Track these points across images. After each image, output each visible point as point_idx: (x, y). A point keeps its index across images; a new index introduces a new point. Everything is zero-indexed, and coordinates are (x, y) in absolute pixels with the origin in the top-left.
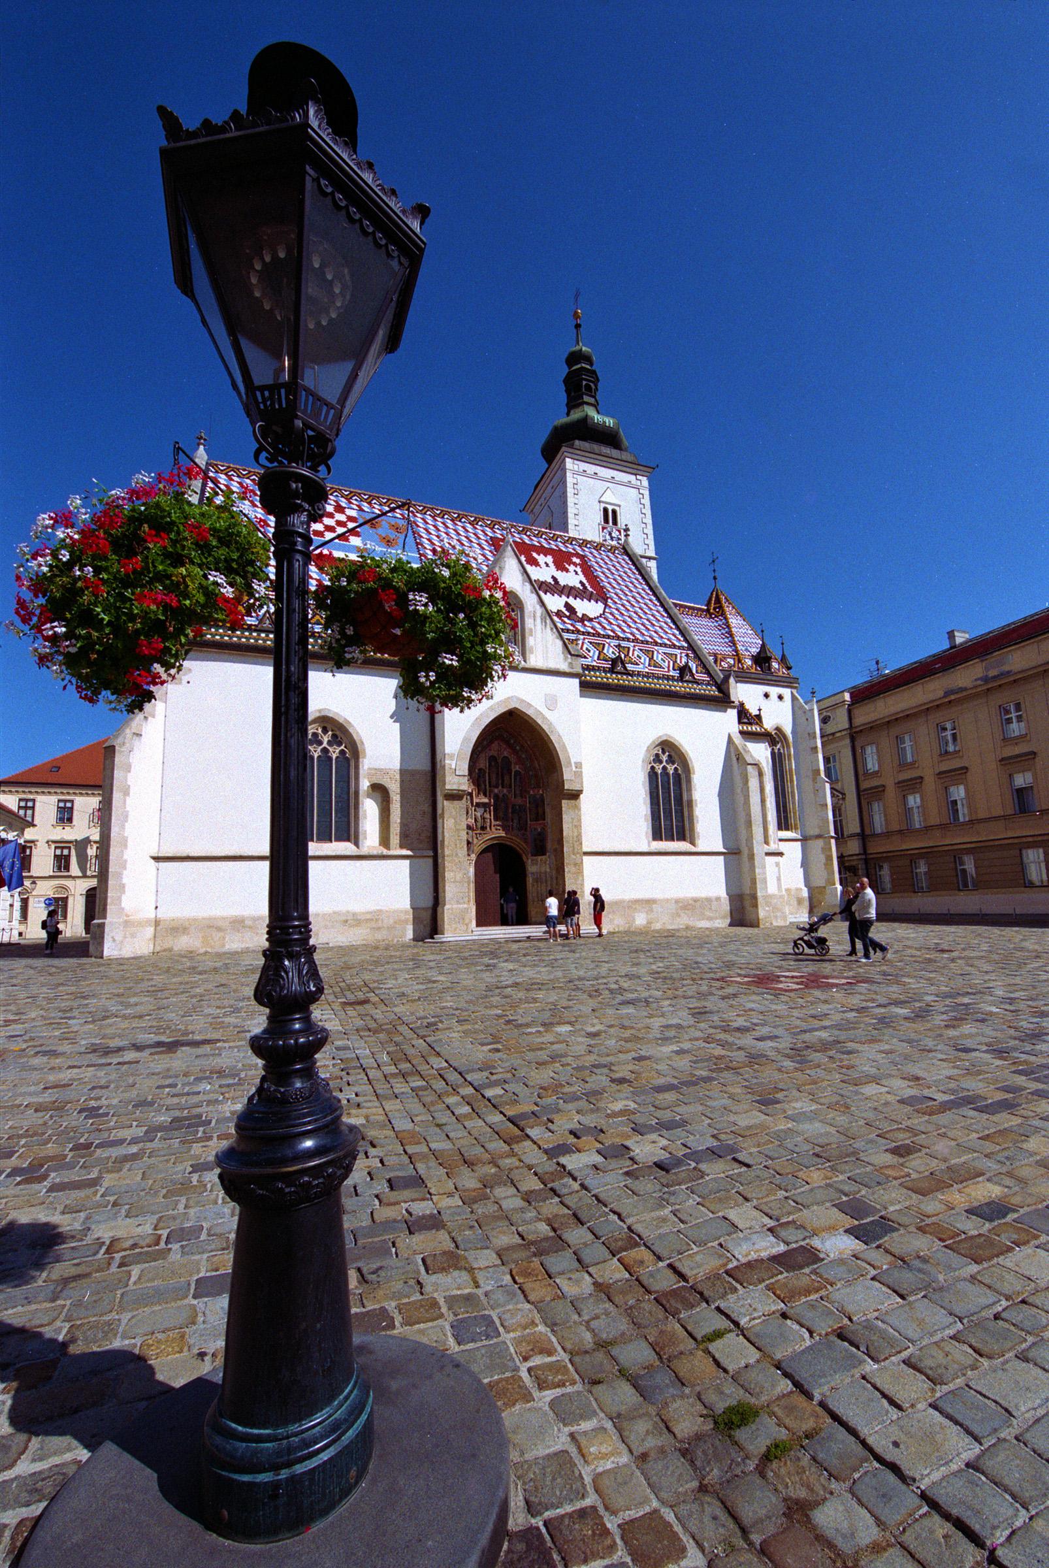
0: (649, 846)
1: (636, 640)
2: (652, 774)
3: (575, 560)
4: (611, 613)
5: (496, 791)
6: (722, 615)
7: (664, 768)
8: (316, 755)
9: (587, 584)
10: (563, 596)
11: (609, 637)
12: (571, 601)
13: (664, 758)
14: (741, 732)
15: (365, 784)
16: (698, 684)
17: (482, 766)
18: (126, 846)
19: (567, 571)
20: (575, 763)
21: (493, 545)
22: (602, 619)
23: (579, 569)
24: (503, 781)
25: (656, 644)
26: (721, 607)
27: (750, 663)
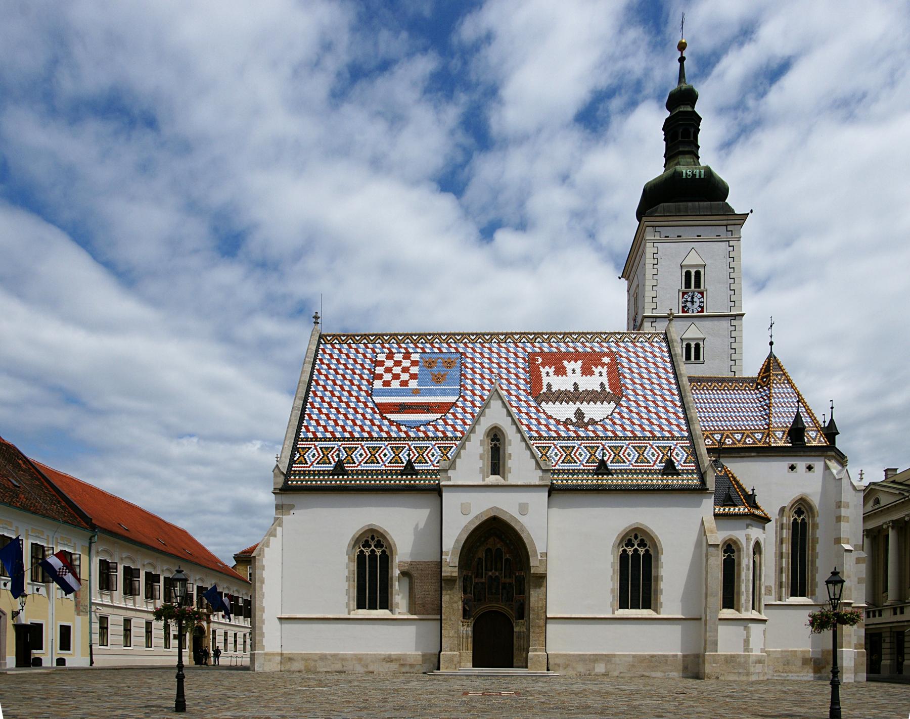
1: (635, 437)
3: (606, 360)
4: (619, 413)
5: (490, 573)
6: (766, 386)
8: (367, 554)
9: (607, 386)
10: (578, 403)
11: (607, 438)
12: (585, 407)
14: (716, 516)
15: (396, 572)
16: (678, 474)
17: (480, 556)
19: (592, 373)
20: (541, 553)
22: (607, 421)
23: (604, 370)
25: (654, 437)
26: (768, 377)
27: (779, 434)
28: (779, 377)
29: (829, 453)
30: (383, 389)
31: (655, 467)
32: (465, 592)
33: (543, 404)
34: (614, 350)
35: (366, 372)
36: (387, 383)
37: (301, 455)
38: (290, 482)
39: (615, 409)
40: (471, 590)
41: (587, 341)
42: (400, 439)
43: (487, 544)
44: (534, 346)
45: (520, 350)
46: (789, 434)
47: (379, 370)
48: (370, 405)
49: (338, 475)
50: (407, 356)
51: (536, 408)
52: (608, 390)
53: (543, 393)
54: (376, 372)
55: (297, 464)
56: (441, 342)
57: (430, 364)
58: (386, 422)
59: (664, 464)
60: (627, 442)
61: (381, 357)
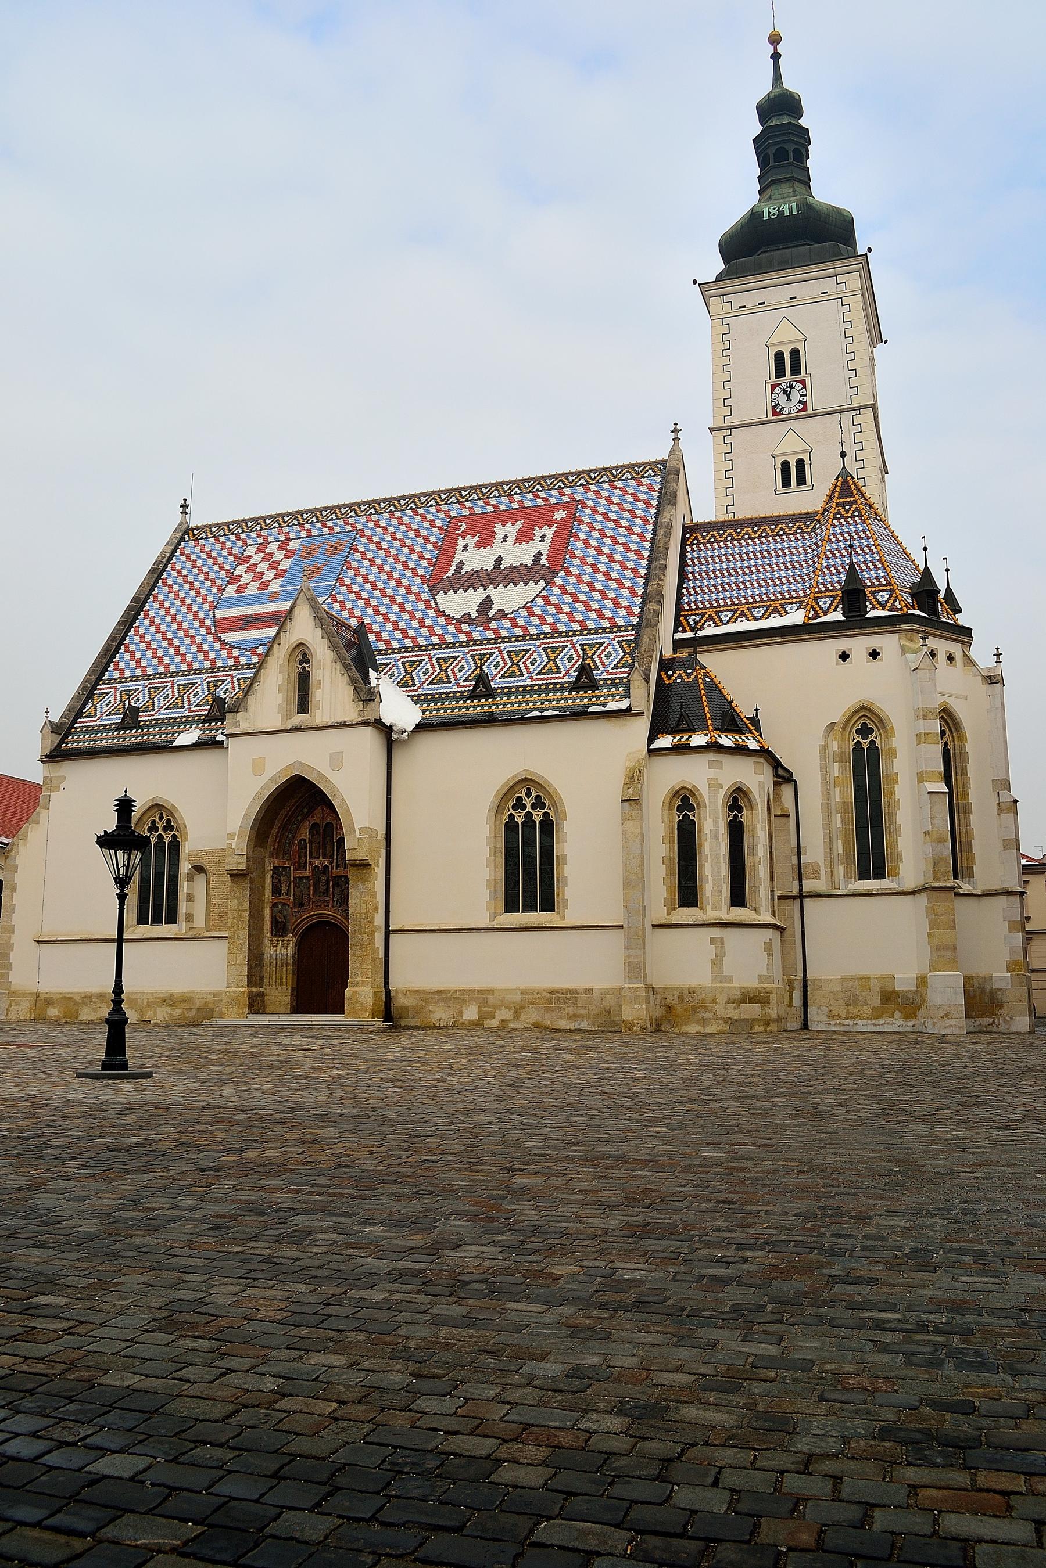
0: (493, 916)
1: (555, 633)
2: (511, 826)
3: (560, 515)
7: (529, 815)
11: (510, 639)
13: (528, 802)
18: (13, 933)
20: (360, 829)
21: (445, 532)
22: (524, 612)
23: (549, 532)
24: (325, 848)
25: (584, 631)
28: (847, 507)
29: (904, 627)
30: (238, 597)
31: (566, 679)
32: (276, 891)
33: (440, 596)
34: (578, 497)
35: (223, 574)
36: (242, 588)
37: (93, 705)
38: (64, 745)
39: (541, 592)
40: (289, 890)
41: (543, 490)
42: (225, 668)
43: (313, 817)
44: (463, 507)
45: (442, 515)
46: (842, 601)
47: (241, 570)
48: (208, 622)
49: (125, 729)
50: (284, 545)
51: (427, 602)
52: (544, 562)
53: (448, 577)
54: (235, 574)
55: (86, 717)
56: (337, 518)
57: (310, 552)
58: (217, 646)
59: (576, 674)
60: (538, 642)
61: (250, 551)
